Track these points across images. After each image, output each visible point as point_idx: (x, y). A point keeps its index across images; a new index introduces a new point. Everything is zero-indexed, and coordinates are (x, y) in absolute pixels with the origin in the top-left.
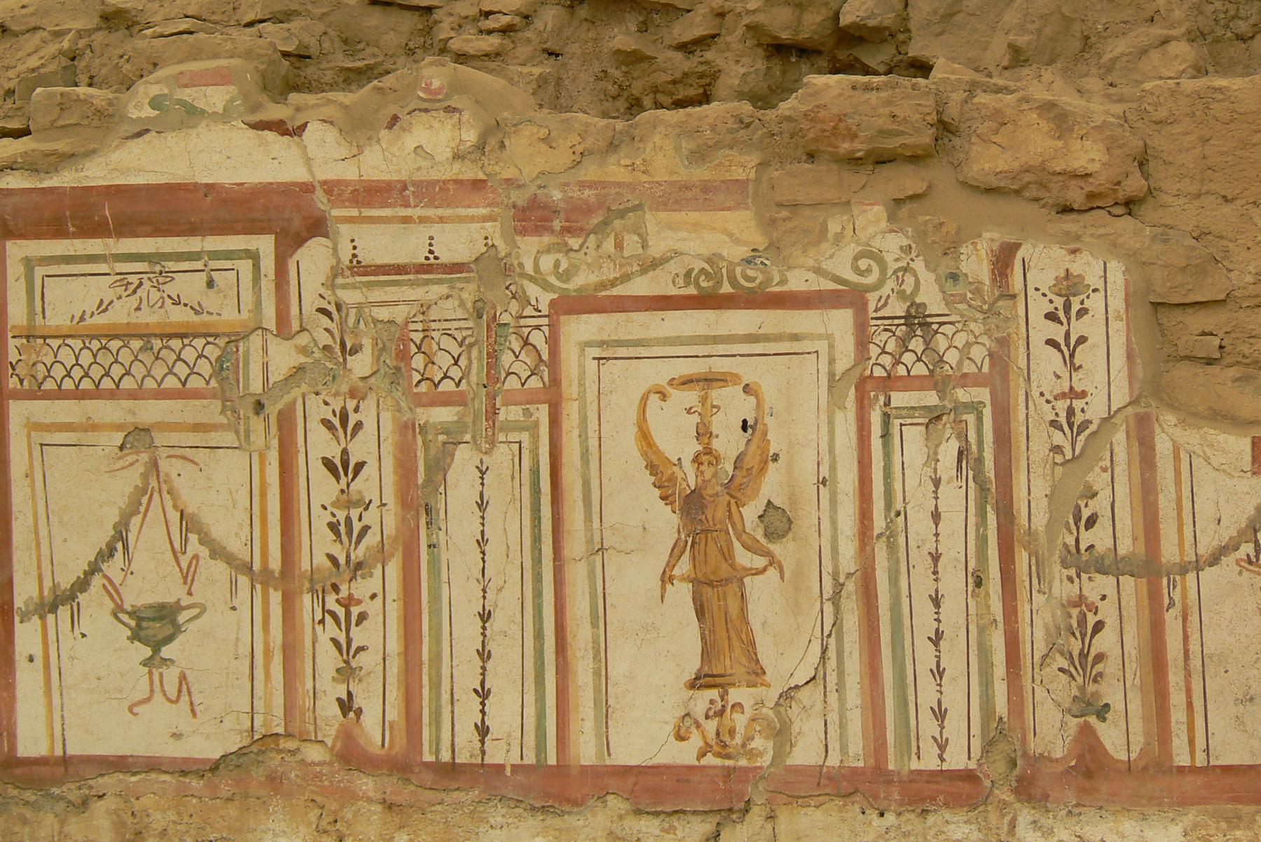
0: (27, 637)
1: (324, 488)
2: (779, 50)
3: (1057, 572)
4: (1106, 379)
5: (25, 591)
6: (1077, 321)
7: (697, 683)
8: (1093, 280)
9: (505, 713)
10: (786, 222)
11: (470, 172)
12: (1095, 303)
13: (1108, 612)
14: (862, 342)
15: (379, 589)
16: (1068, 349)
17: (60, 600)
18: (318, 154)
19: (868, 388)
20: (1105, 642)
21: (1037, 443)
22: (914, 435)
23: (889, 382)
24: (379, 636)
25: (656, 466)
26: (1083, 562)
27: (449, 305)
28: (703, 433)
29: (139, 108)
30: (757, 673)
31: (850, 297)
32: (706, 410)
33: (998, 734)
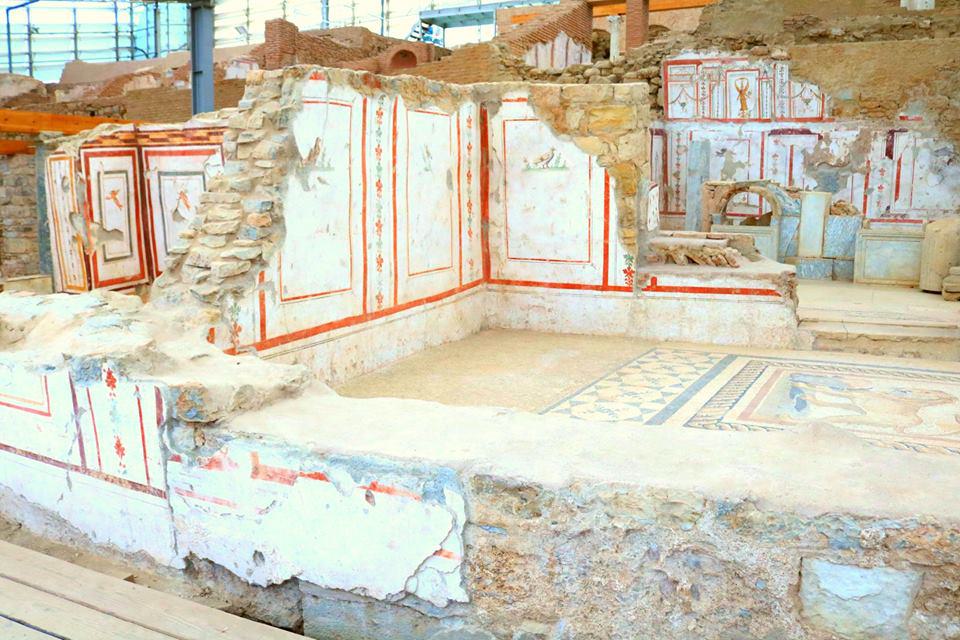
0: (670, 107)
1: (701, 90)
2: (749, 43)
4: (786, 77)
5: (669, 101)
6: (783, 70)
7: (742, 109)
9: (720, 113)
10: (751, 62)
15: (707, 101)
16: (782, 75)
18: (702, 56)
21: (778, 85)
24: (707, 105)
25: (737, 89)
26: (782, 97)
27: (715, 72)
29: (682, 51)
31: (758, 70)
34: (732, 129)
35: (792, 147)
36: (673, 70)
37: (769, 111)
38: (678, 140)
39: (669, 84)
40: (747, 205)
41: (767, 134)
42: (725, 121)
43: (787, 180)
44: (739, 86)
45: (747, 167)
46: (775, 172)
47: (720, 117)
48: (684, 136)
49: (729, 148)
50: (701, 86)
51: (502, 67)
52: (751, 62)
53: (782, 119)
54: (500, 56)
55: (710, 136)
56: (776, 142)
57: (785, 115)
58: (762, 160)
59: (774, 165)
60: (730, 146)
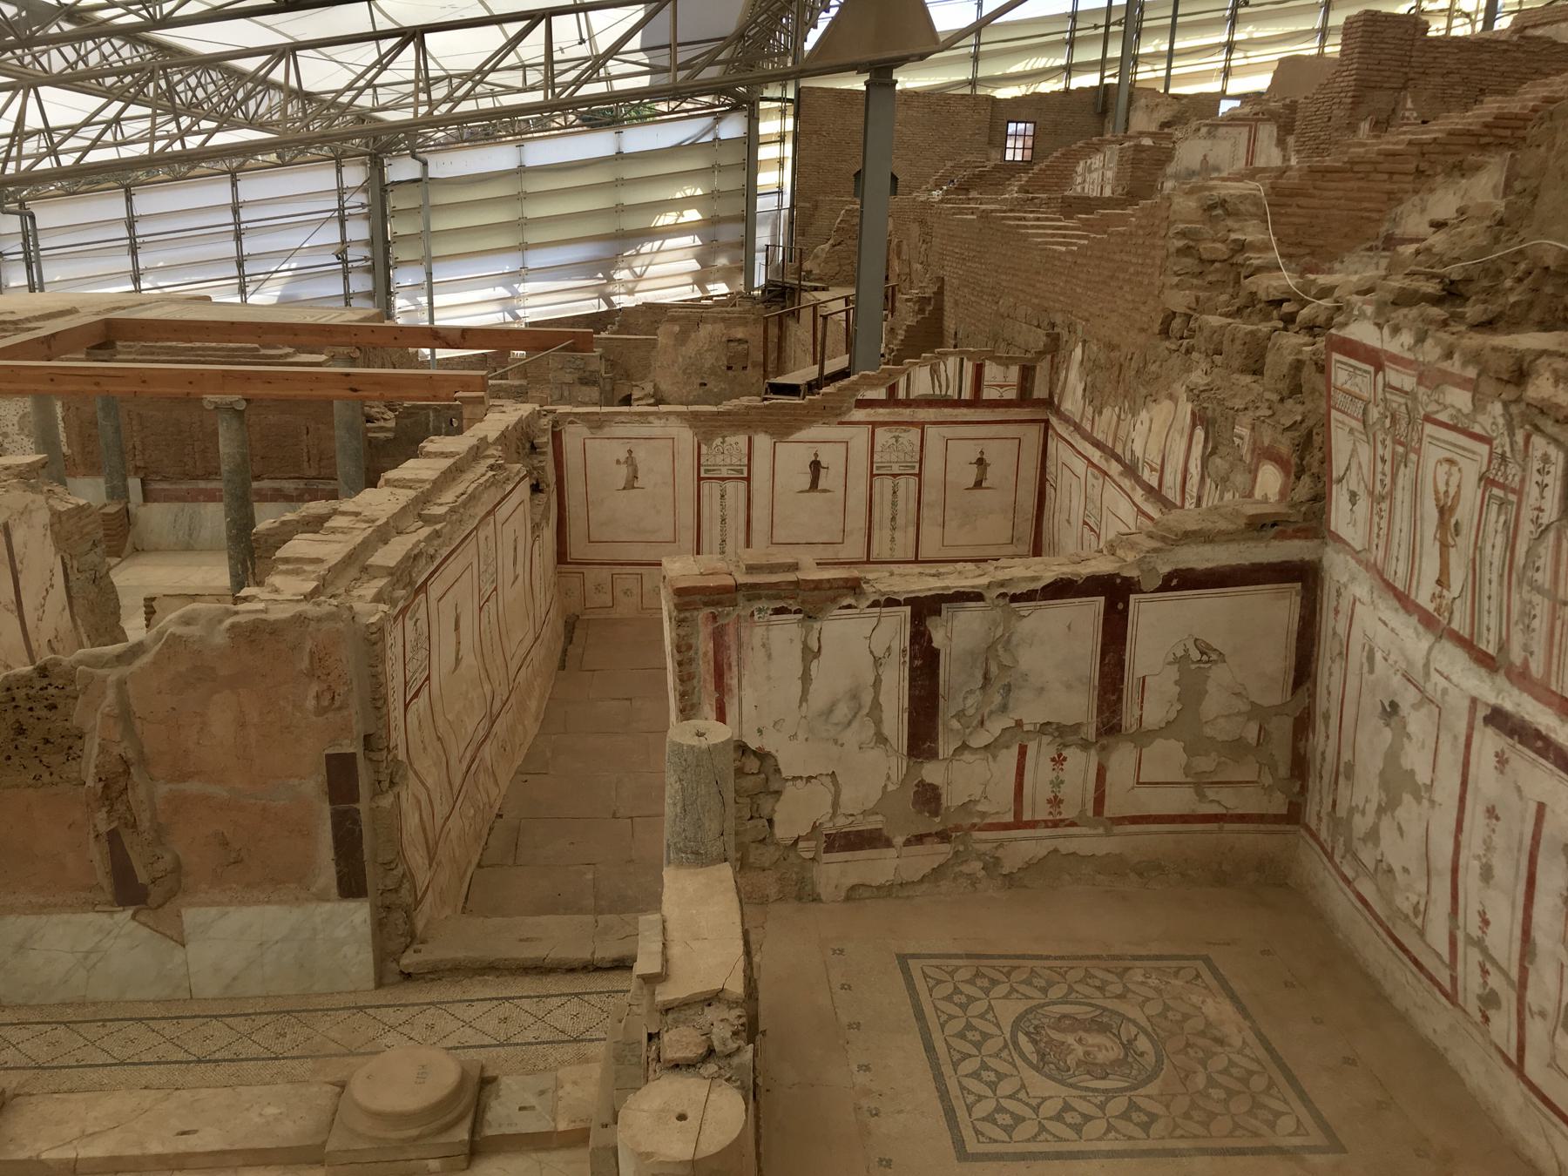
3: (1526, 588)
7: (1439, 582)
8: (1553, 459)
11: (1409, 356)
12: (1552, 469)
13: (1537, 611)
14: (1490, 462)
16: (1543, 487)
17: (1340, 480)
19: (1486, 481)
20: (1536, 623)
21: (1526, 528)
22: (1495, 508)
23: (1493, 483)
24: (1384, 524)
25: (1436, 492)
28: (1447, 484)
30: (1448, 587)
32: (1449, 474)
33: (1503, 647)
34: (1414, 642)
35: (1541, 807)
36: (1343, 373)
37: (1493, 624)
38: (1337, 612)
39: (1333, 412)
40: (1421, 933)
41: (1482, 712)
42: (1404, 601)
43: (1518, 932)
44: (1442, 488)
45: (1425, 802)
46: (1487, 874)
47: (1399, 585)
48: (1345, 605)
49: (1405, 708)
50: (1380, 451)
51: (1188, 261)
52: (1478, 405)
53: (1521, 678)
54: (1182, 234)
55: (1381, 637)
56: (1502, 760)
57: (1536, 668)
58: (1462, 799)
59: (1489, 846)
60: (1407, 698)
